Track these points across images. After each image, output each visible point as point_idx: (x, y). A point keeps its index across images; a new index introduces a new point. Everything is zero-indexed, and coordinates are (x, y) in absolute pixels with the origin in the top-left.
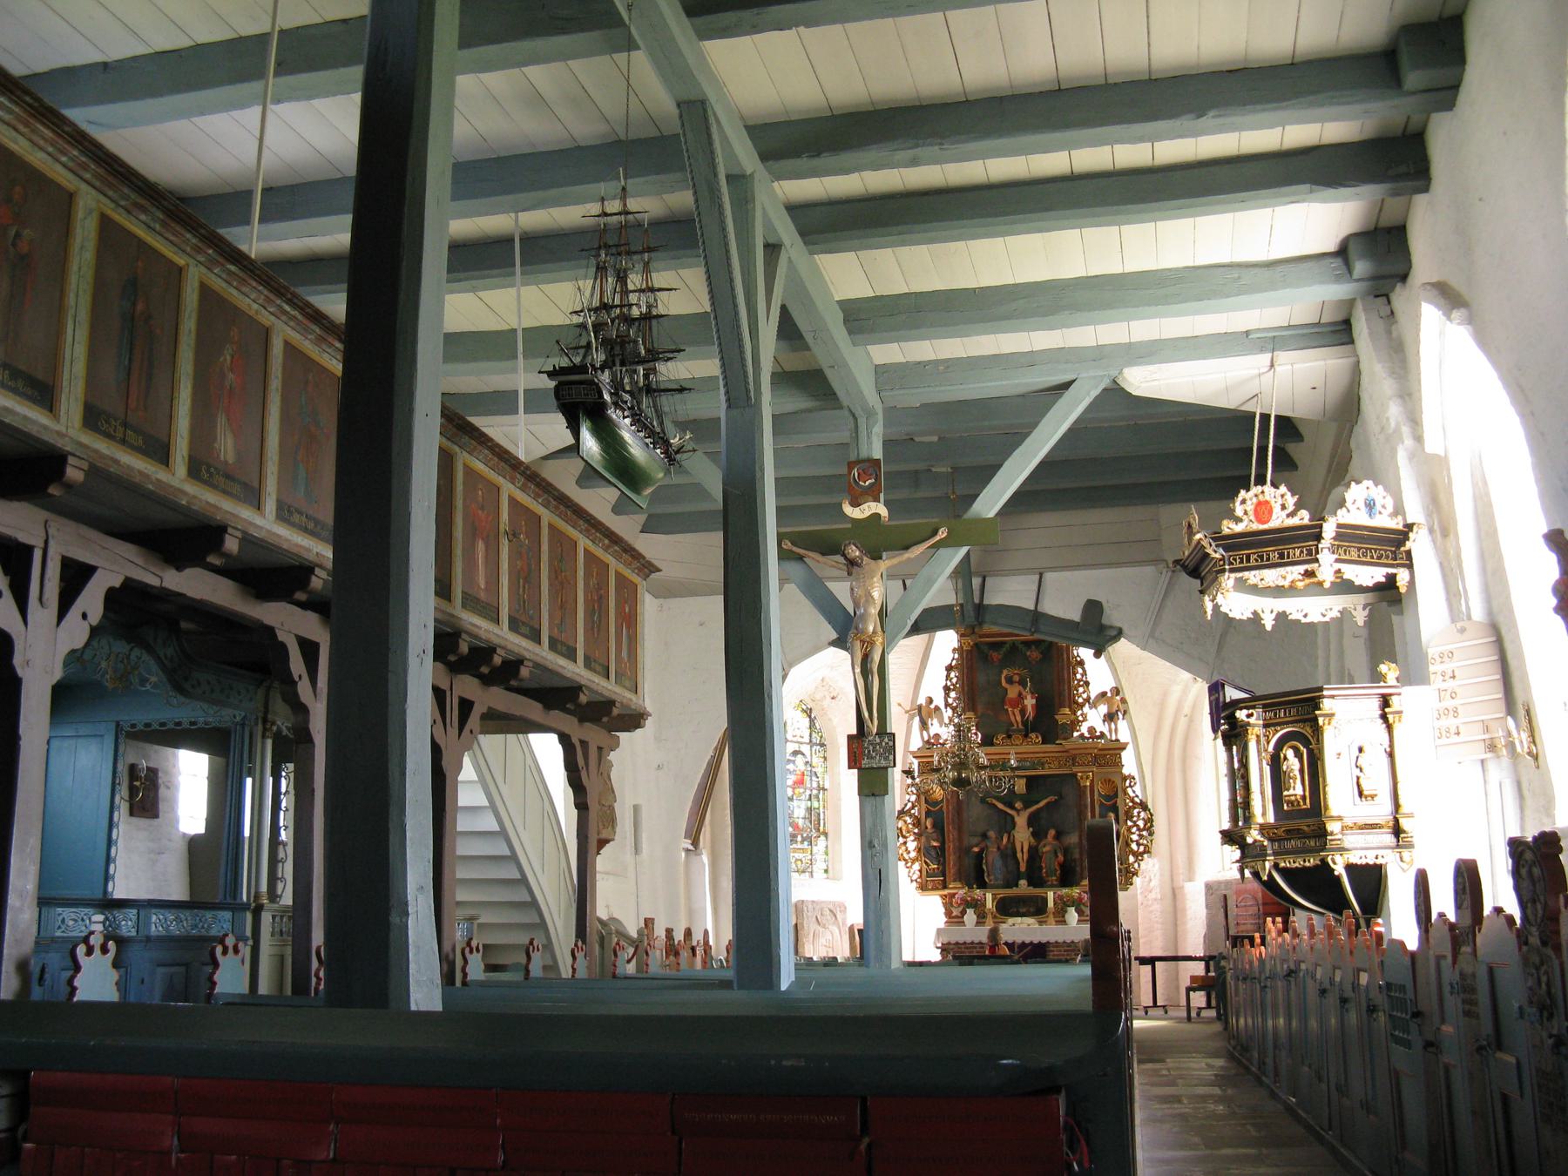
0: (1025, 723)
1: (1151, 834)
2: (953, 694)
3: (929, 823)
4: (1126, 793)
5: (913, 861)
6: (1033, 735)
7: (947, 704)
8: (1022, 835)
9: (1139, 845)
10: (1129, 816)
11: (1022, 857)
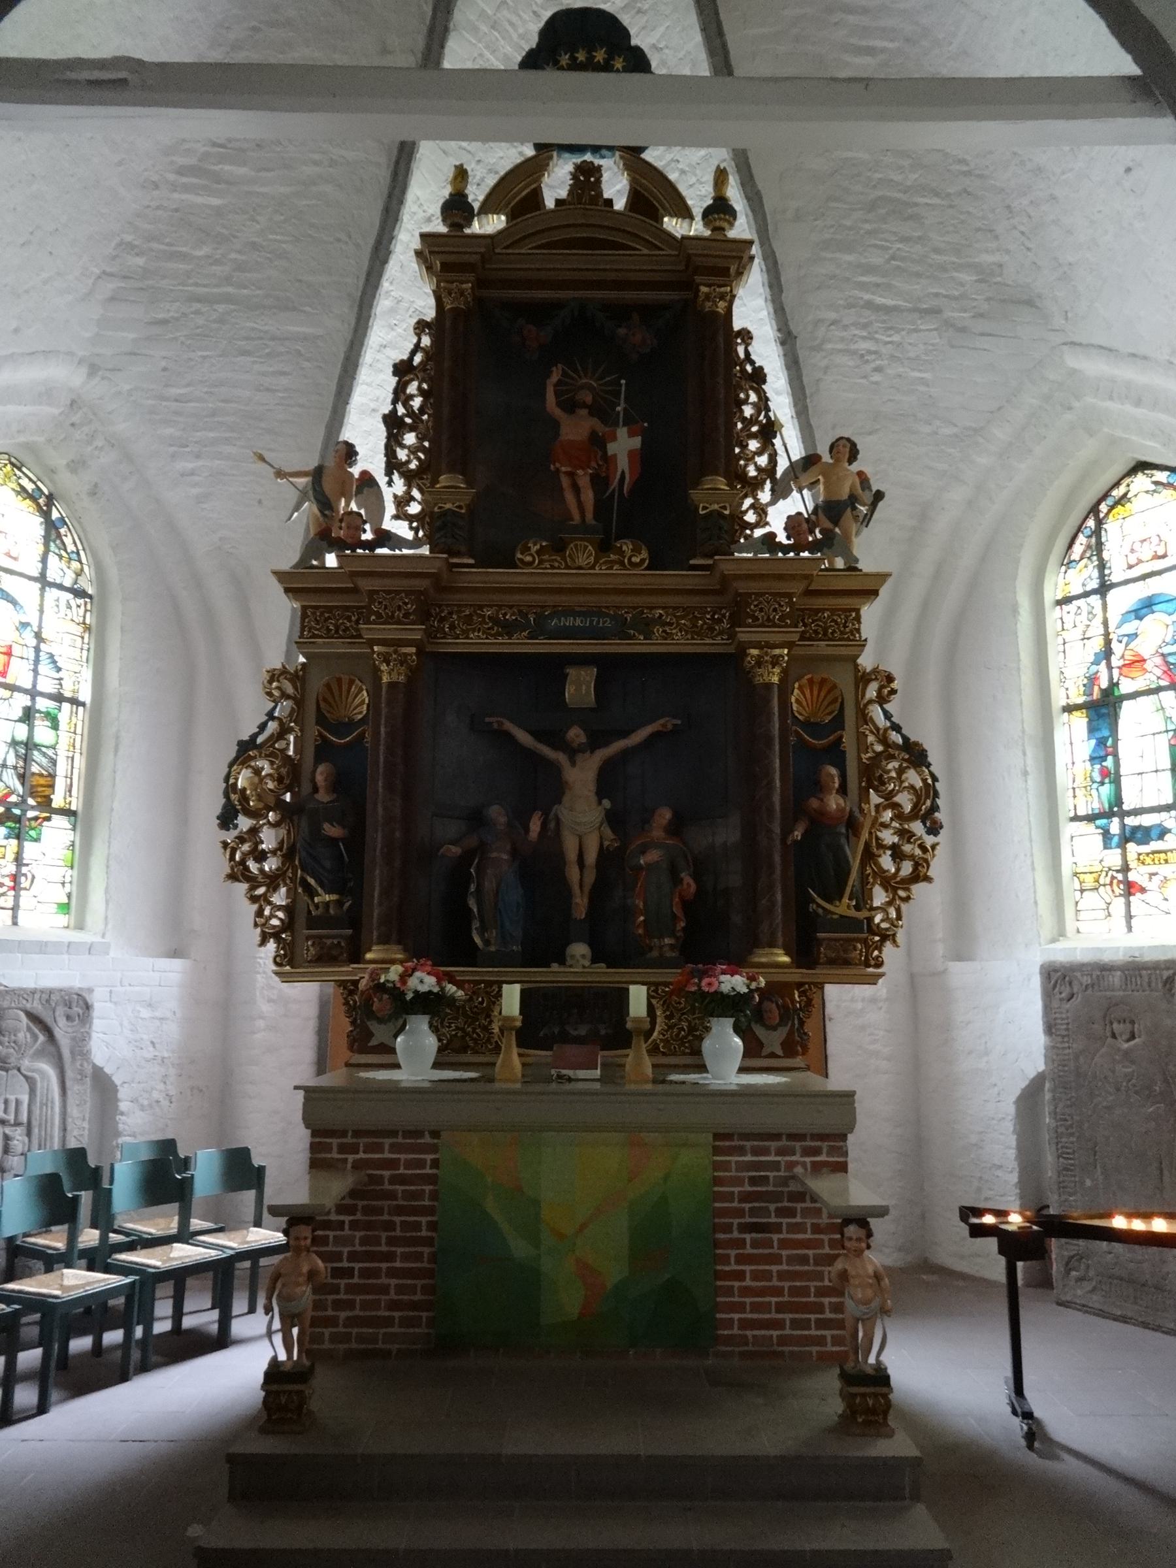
0: (602, 507)
1: (934, 829)
2: (410, 439)
3: (321, 774)
4: (863, 717)
5: (273, 881)
6: (627, 547)
7: (392, 465)
8: (582, 819)
9: (897, 854)
10: (872, 776)
11: (579, 882)
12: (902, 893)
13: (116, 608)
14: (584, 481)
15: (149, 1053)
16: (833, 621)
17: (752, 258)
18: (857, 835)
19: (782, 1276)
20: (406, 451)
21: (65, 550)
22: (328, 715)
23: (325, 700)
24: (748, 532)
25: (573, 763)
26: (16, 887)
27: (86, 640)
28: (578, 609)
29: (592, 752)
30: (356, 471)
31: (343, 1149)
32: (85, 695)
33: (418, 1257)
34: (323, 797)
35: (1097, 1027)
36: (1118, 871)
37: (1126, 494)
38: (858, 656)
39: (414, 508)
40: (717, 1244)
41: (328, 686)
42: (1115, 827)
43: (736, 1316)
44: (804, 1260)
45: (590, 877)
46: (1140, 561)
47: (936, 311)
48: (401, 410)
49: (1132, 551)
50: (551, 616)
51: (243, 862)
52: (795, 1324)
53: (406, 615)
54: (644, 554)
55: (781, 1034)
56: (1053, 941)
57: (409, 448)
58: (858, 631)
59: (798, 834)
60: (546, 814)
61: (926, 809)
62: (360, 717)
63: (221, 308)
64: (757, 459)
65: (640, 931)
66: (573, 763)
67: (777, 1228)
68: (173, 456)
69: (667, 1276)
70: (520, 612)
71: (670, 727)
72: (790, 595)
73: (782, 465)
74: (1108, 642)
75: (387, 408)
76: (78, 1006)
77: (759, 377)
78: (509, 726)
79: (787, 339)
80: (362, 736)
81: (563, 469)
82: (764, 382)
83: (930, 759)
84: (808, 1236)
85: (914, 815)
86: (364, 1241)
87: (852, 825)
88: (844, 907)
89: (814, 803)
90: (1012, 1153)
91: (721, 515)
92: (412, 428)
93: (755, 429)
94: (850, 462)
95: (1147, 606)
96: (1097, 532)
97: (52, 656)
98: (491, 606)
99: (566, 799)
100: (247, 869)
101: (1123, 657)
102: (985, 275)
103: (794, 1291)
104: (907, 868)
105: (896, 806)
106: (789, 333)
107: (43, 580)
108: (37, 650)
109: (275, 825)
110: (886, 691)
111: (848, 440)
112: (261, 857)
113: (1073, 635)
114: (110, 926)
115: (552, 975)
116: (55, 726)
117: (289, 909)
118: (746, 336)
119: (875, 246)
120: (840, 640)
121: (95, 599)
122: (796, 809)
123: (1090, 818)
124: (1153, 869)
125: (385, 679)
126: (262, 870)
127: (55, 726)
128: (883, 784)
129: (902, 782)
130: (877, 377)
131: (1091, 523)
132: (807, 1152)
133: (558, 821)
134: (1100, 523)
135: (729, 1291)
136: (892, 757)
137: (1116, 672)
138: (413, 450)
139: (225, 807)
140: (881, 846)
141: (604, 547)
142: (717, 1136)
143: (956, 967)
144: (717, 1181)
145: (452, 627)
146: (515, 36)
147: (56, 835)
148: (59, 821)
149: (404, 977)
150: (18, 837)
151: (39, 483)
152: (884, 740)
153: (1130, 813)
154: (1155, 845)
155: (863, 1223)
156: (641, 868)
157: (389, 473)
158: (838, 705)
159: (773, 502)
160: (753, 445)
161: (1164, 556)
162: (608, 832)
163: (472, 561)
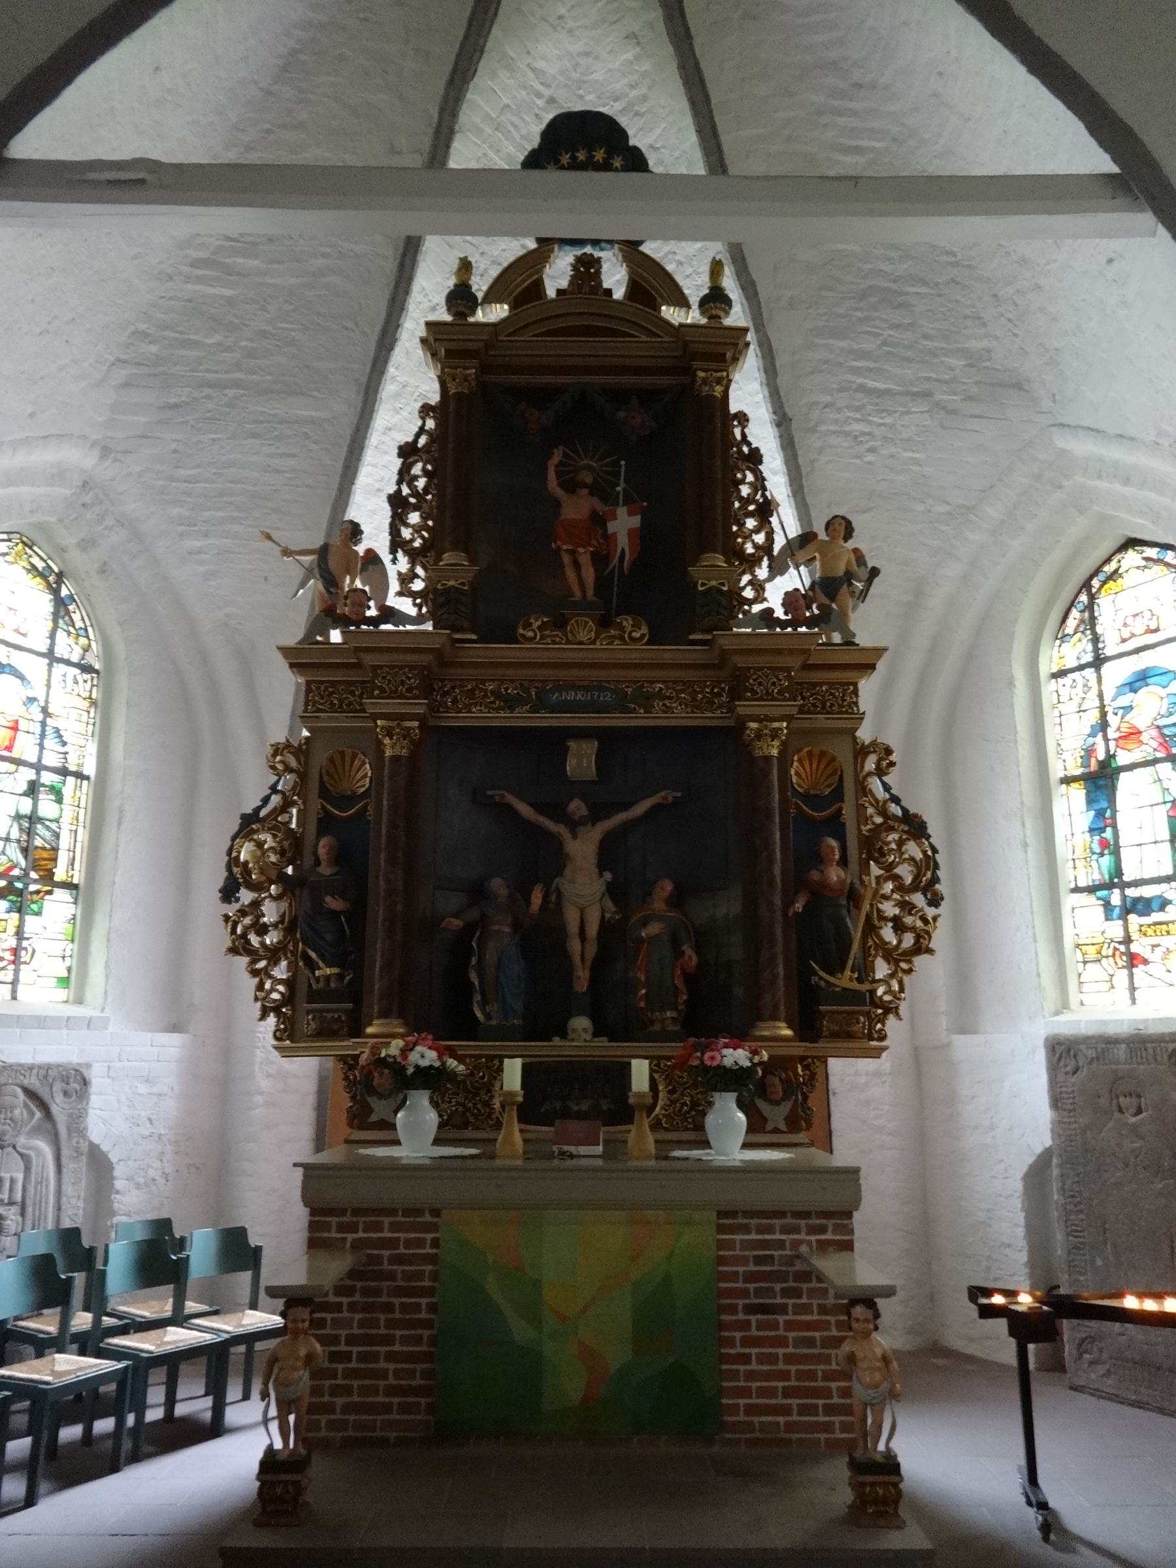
0: (602, 584)
2: (414, 518)
3: (324, 847)
4: (863, 789)
5: (273, 955)
6: (627, 622)
7: (397, 543)
8: (584, 891)
9: (899, 927)
10: (872, 848)
11: (580, 953)
12: (904, 965)
13: (123, 683)
14: (585, 559)
15: (146, 1129)
16: (832, 694)
17: (747, 345)
18: (858, 907)
19: (789, 1359)
20: (410, 530)
21: (74, 626)
22: (330, 788)
23: (329, 774)
24: (746, 607)
25: (575, 836)
26: (16, 962)
27: (92, 715)
28: (578, 683)
29: (593, 825)
30: (361, 549)
31: (342, 1228)
32: (90, 769)
33: (418, 1340)
34: (325, 870)
35: (1103, 1101)
36: (1120, 943)
37: (1116, 571)
38: (856, 729)
39: (418, 585)
40: (721, 1326)
41: (331, 760)
42: (1116, 898)
43: (742, 1402)
44: (810, 1342)
45: (592, 950)
46: (1133, 635)
47: (927, 395)
48: (406, 490)
49: (1125, 625)
50: (552, 691)
51: (244, 936)
52: (804, 1410)
53: (409, 690)
54: (644, 630)
55: (786, 1108)
56: (1057, 1013)
57: (413, 526)
58: (856, 704)
59: (799, 906)
60: (547, 886)
61: (926, 880)
62: (363, 790)
63: (230, 393)
64: (754, 537)
65: (642, 1004)
66: (575, 836)
67: (783, 1309)
68: (182, 535)
69: (671, 1360)
70: (521, 685)
71: (670, 799)
72: (788, 670)
73: (779, 543)
74: (1104, 715)
75: (392, 489)
76: (76, 1082)
77: (755, 458)
78: (510, 799)
79: (782, 421)
80: (365, 808)
81: (565, 547)
82: (761, 462)
83: (930, 831)
84: (815, 1317)
85: (915, 887)
86: (362, 1324)
87: (854, 897)
88: (846, 980)
89: (815, 875)
90: (1020, 1231)
91: (720, 591)
92: (416, 508)
93: (752, 508)
94: (846, 539)
95: (1140, 680)
96: (1090, 607)
97: (57, 731)
98: (493, 680)
99: (567, 872)
100: (248, 942)
101: (1118, 729)
102: (974, 360)
103: (801, 1375)
104: (909, 940)
105: (896, 878)
106: (785, 415)
107: (51, 656)
108: (43, 724)
109: (277, 898)
110: (884, 763)
111: (844, 518)
112: (262, 930)
113: (1069, 707)
114: (109, 1000)
115: (554, 1049)
116: (59, 800)
117: (290, 983)
118: (742, 418)
119: (867, 332)
120: (838, 713)
121: (101, 675)
122: (797, 881)
123: (1091, 890)
124: (1155, 940)
125: (388, 753)
126: (263, 944)
127: (59, 800)
128: (883, 855)
129: (903, 853)
130: (870, 458)
131: (1084, 598)
132: (812, 1230)
133: (559, 894)
134: (1092, 598)
135: (734, 1375)
136: (891, 829)
137: (1112, 744)
138: (417, 529)
139: (227, 879)
140: (882, 918)
141: (605, 623)
142: (721, 1214)
143: (960, 1040)
144: (722, 1261)
145: (455, 701)
146: (517, 137)
147: (58, 909)
148: (61, 894)
149: (405, 1051)
150: (19, 911)
151: (49, 562)
152: (883, 812)
153: (1130, 885)
154: (1156, 917)
155: (870, 1304)
156: (640, 941)
157: (393, 551)
158: (837, 778)
159: (770, 579)
160: (751, 523)
161: (1157, 630)
162: (609, 904)
163: (474, 637)
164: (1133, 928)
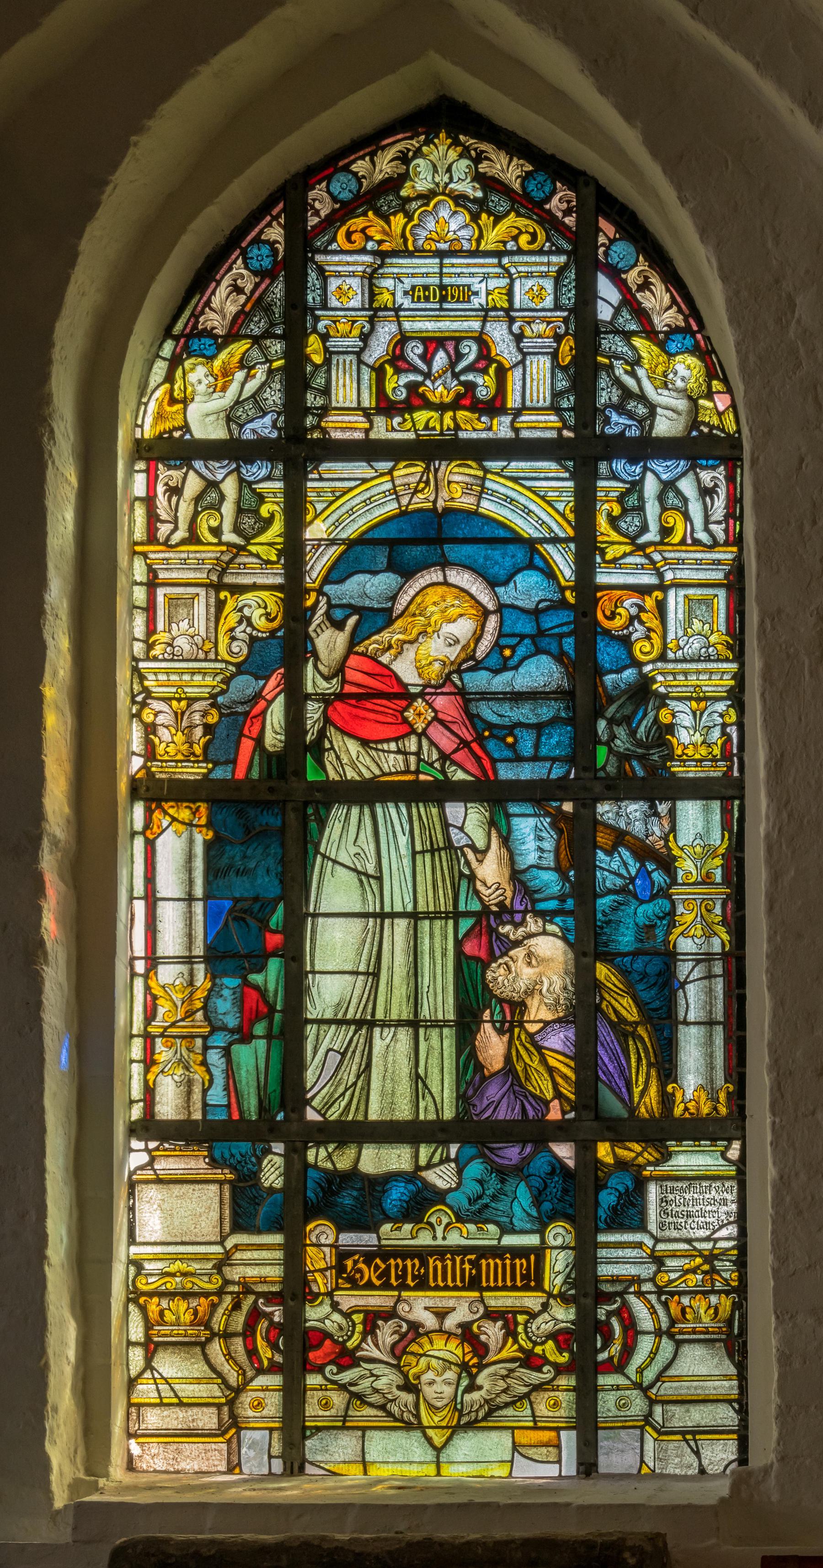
36: (271, 1298)
37: (393, 184)
42: (272, 1174)
46: (416, 399)
49: (397, 359)
95: (419, 542)
101: (340, 670)
124: (378, 1300)
137: (313, 711)
154: (396, 1235)
161: (494, 407)
164: (317, 1259)
